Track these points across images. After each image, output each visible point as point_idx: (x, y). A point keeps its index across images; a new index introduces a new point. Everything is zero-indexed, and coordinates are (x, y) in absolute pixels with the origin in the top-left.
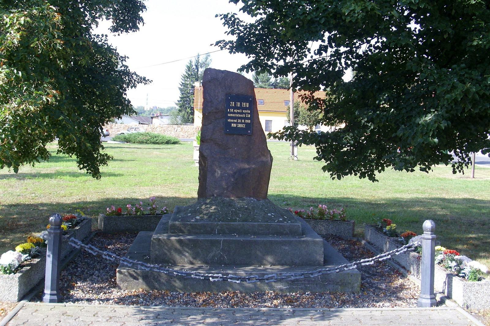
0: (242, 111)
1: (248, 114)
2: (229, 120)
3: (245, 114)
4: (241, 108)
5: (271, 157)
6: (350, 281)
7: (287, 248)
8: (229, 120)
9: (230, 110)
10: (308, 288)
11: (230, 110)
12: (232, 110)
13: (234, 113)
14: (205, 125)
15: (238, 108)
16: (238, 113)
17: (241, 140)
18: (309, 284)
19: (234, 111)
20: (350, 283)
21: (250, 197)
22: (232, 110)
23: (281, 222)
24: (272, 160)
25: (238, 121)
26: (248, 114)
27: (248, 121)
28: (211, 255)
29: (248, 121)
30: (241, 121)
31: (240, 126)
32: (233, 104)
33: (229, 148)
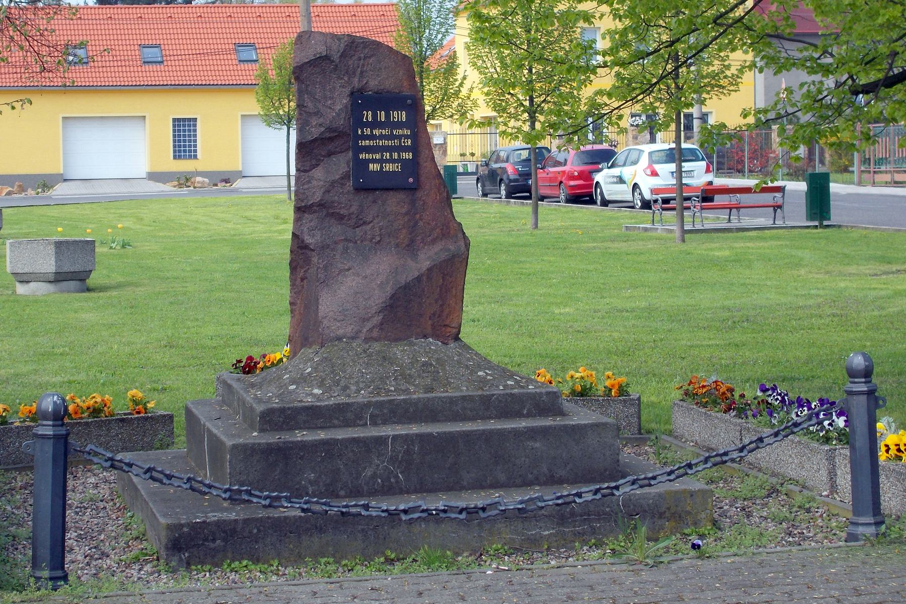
0: (392, 132)
1: (407, 137)
3: (399, 137)
5: (465, 238)
6: (689, 508)
7: (538, 445)
9: (363, 132)
10: (597, 531)
11: (363, 132)
12: (367, 131)
13: (372, 137)
14: (305, 171)
15: (381, 125)
16: (381, 137)
17: (394, 203)
18: (599, 520)
19: (372, 132)
20: (689, 513)
21: (425, 337)
22: (367, 131)
23: (512, 387)
24: (467, 245)
25: (382, 156)
26: (407, 137)
27: (408, 156)
28: (369, 472)
29: (408, 156)
30: (391, 156)
31: (389, 167)
32: (370, 116)
33: (365, 223)
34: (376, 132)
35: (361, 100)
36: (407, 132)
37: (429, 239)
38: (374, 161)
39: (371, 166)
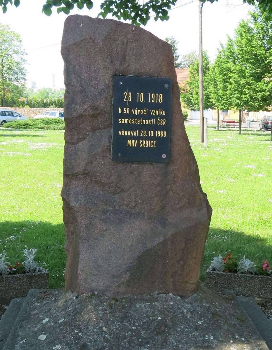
0: (149, 112)
1: (162, 117)
2: (122, 133)
3: (156, 117)
8: (122, 133)
9: (123, 111)
11: (123, 111)
13: (131, 116)
14: (73, 144)
15: (140, 106)
16: (140, 116)
17: (148, 173)
19: (131, 111)
22: (127, 111)
25: (140, 133)
26: (162, 117)
29: (162, 134)
30: (147, 133)
31: (145, 144)
32: (130, 97)
33: (123, 190)
34: (135, 112)
35: (123, 82)
36: (162, 113)
37: (177, 206)
38: (132, 138)
39: (129, 142)
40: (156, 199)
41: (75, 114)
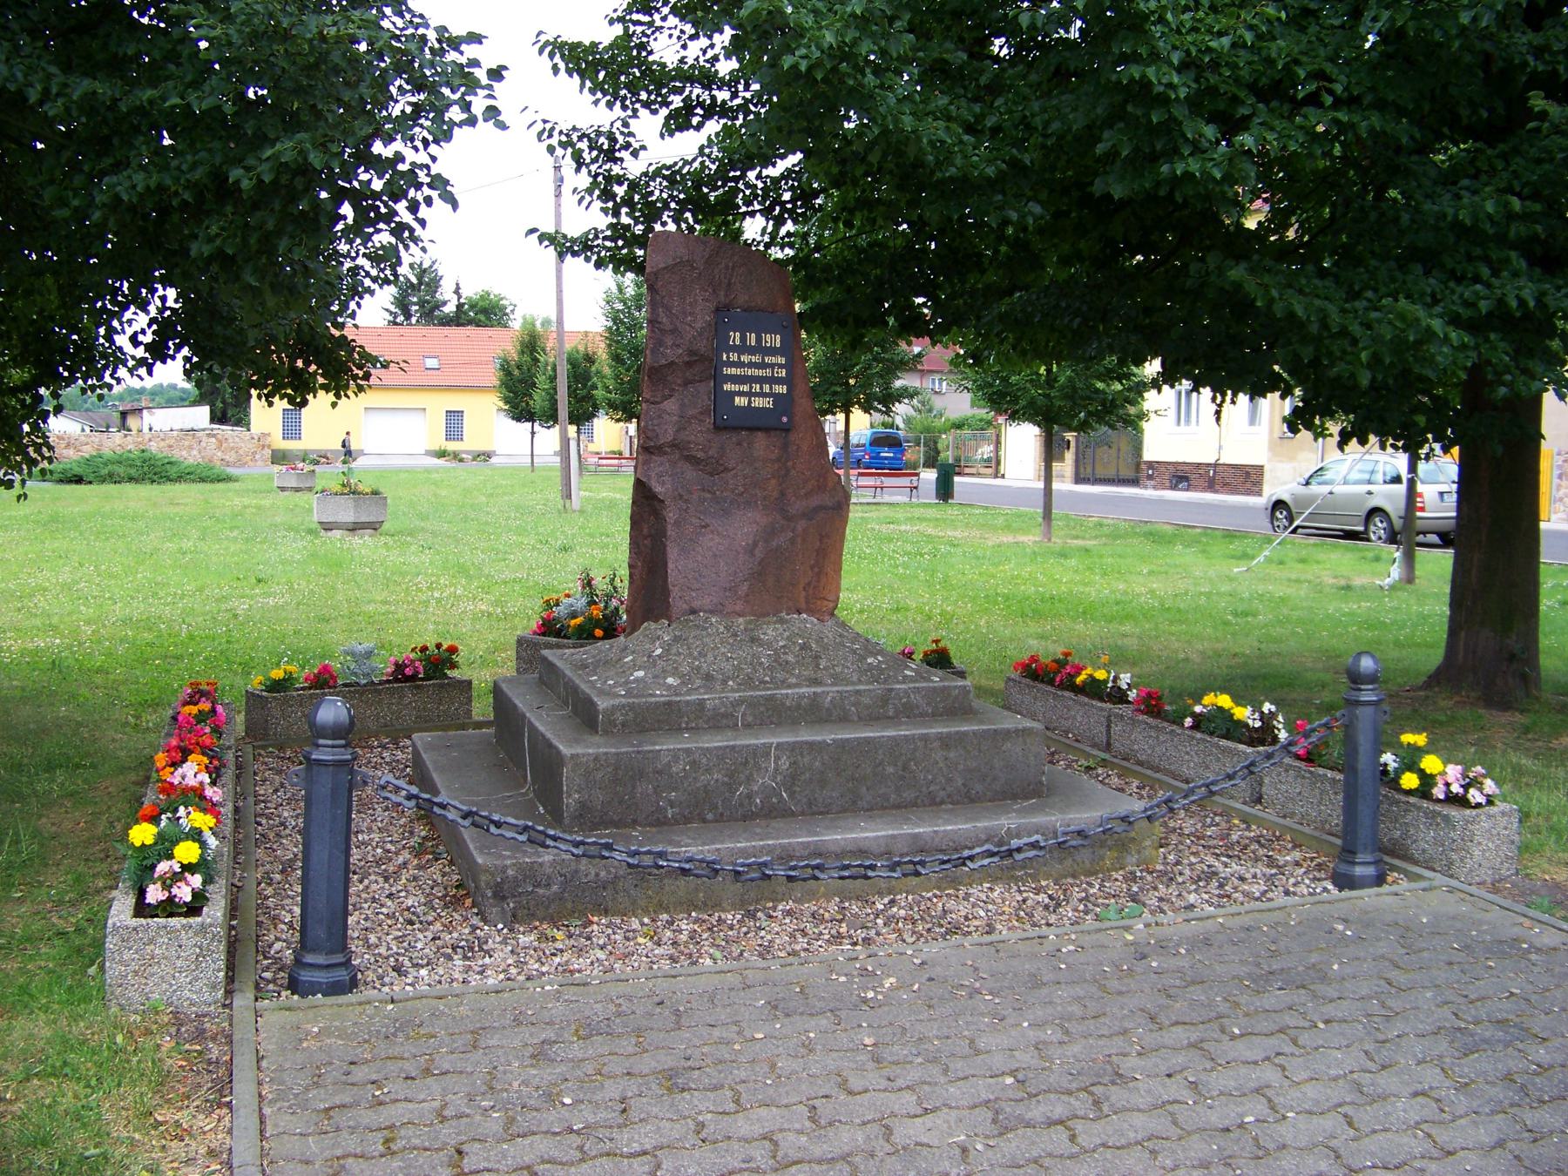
1: (781, 366)
2: (727, 387)
3: (772, 366)
4: (759, 349)
8: (727, 387)
12: (734, 357)
13: (740, 365)
15: (752, 351)
16: (751, 365)
17: (761, 443)
22: (734, 357)
26: (781, 366)
29: (781, 389)
31: (758, 402)
33: (726, 470)
34: (745, 358)
37: (802, 492)
38: (741, 394)
40: (773, 482)
41: (664, 362)
